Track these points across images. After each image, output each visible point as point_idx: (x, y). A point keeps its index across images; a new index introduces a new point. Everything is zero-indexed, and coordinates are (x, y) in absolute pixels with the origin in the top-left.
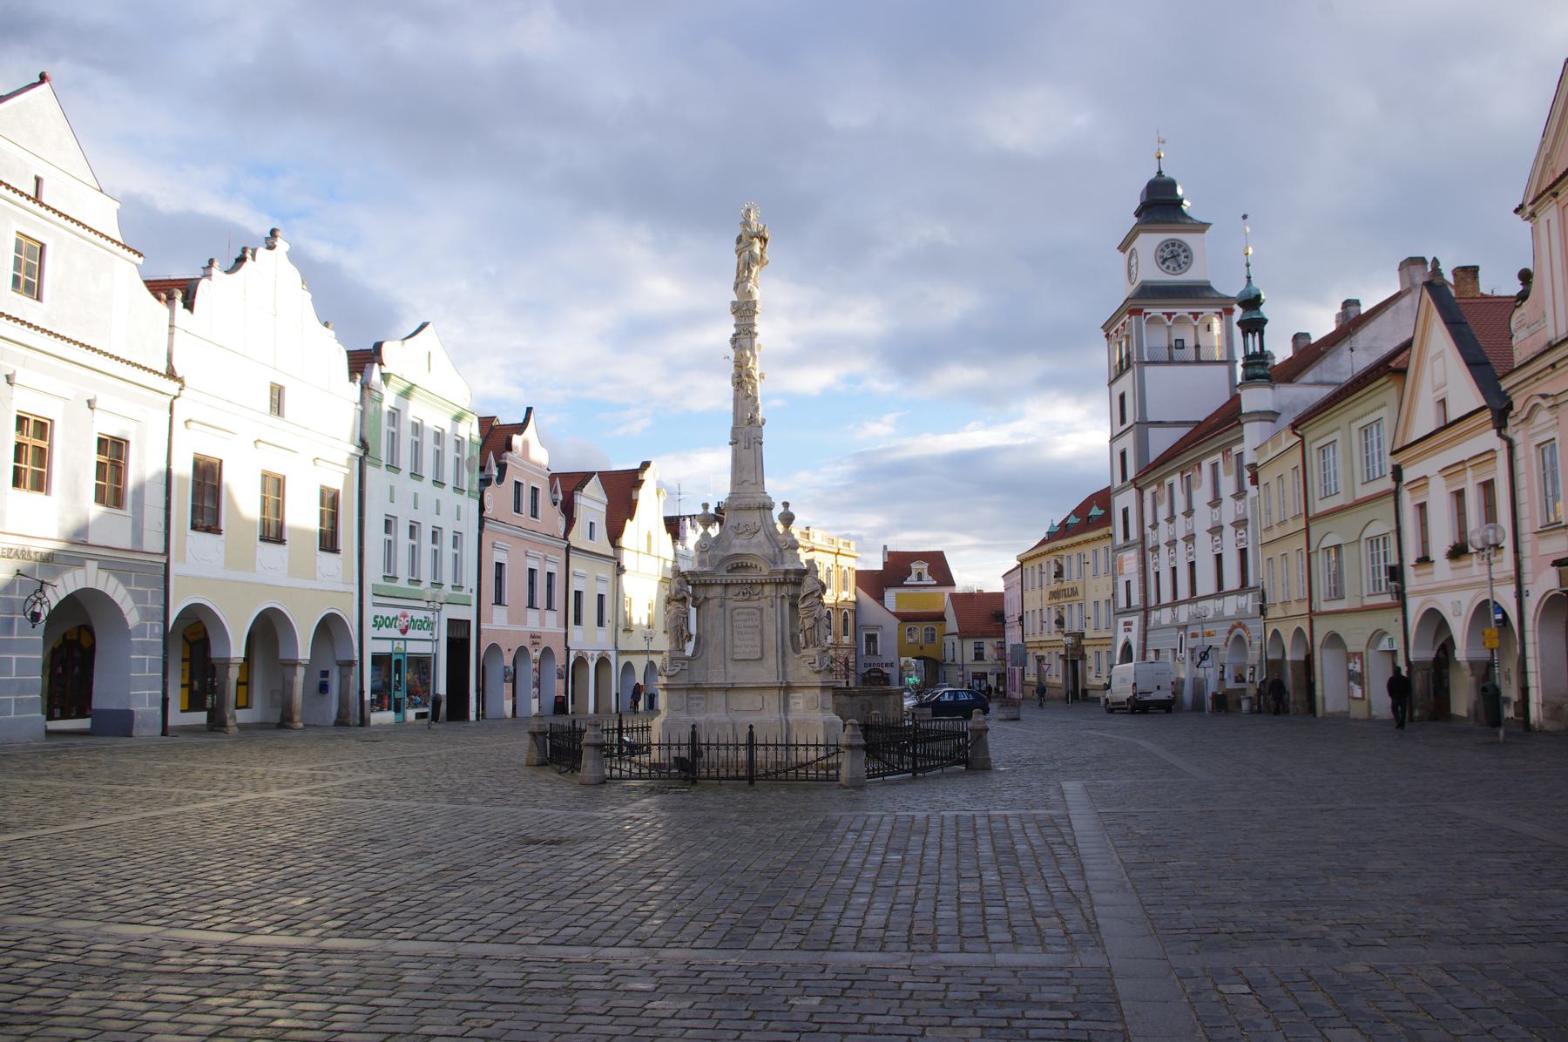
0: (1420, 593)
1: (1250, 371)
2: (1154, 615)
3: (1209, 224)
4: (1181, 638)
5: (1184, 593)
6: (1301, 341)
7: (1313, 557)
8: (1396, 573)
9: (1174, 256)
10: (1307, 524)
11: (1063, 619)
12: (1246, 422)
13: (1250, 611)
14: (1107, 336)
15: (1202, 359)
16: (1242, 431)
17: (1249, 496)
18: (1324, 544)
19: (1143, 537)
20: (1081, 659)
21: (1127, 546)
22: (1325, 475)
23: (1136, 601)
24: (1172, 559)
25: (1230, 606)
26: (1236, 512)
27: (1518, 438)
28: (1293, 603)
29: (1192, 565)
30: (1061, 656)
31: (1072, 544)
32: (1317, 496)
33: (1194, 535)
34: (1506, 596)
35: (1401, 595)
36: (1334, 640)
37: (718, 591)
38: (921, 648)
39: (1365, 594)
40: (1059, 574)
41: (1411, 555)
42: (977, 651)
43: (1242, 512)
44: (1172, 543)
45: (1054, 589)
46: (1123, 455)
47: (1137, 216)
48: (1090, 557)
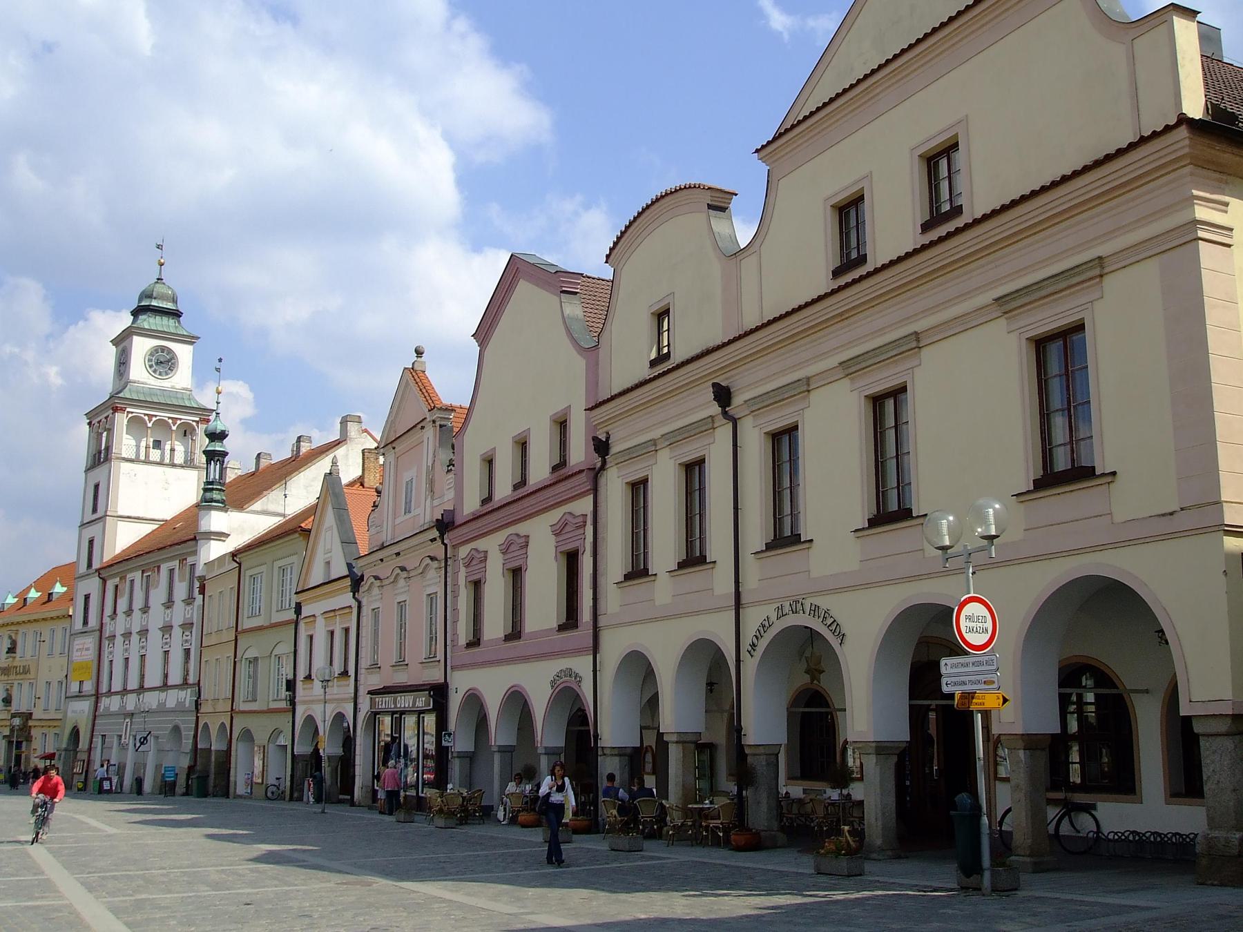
0: (305, 702)
1: (208, 495)
2: (104, 702)
4: (127, 725)
6: (262, 460)
8: (291, 685)
9: (163, 362)
10: (236, 637)
11: (11, 697)
12: (200, 539)
13: (187, 705)
14: (90, 424)
15: (176, 462)
19: (102, 624)
20: (27, 741)
21: (85, 632)
22: (253, 598)
23: (88, 687)
24: (126, 650)
25: (172, 699)
27: (364, 602)
29: (143, 656)
30: (5, 737)
31: (29, 621)
32: (246, 616)
33: (147, 630)
36: (247, 735)
39: (271, 699)
40: (12, 650)
41: (301, 674)
43: (189, 616)
44: (127, 635)
47: (132, 315)
48: (46, 635)
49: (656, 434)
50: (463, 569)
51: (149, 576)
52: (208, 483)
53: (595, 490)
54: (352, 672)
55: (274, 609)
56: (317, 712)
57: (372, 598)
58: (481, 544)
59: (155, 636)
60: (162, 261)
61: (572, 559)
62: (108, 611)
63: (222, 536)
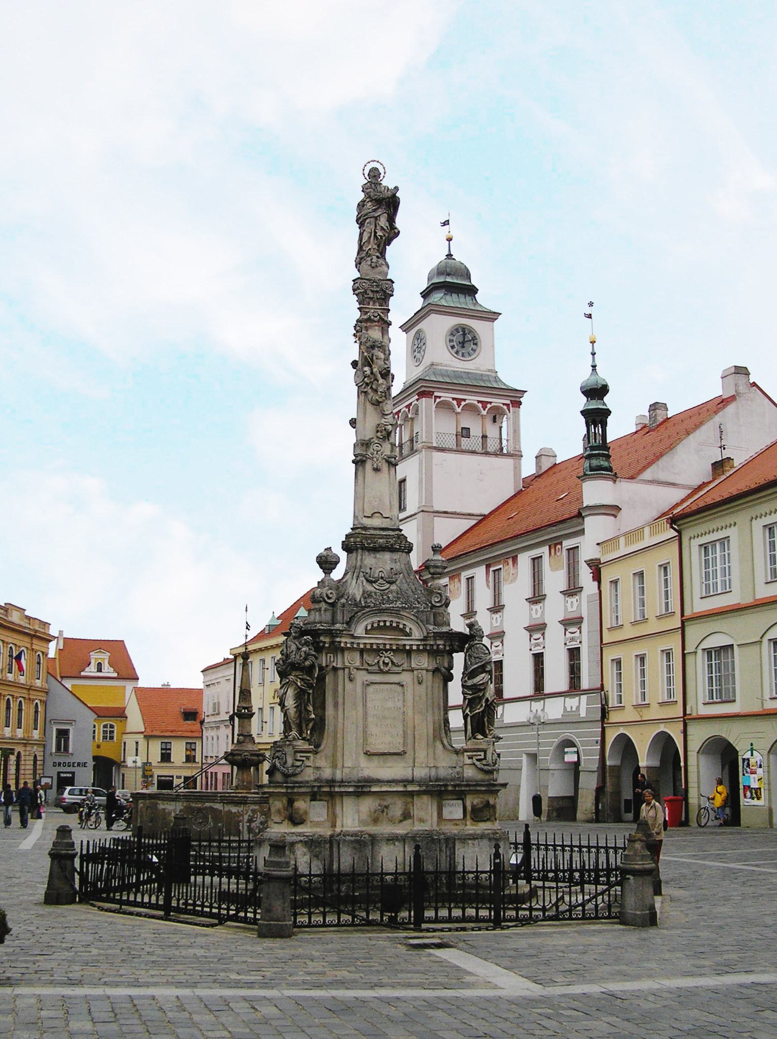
7: (689, 660)
10: (683, 622)
13: (583, 713)
15: (489, 450)
16: (583, 524)
17: (584, 594)
18: (707, 644)
25: (554, 709)
26: (566, 607)
28: (654, 706)
32: (697, 595)
38: (98, 747)
39: (767, 696)
42: (164, 751)
51: (501, 569)
60: (450, 236)
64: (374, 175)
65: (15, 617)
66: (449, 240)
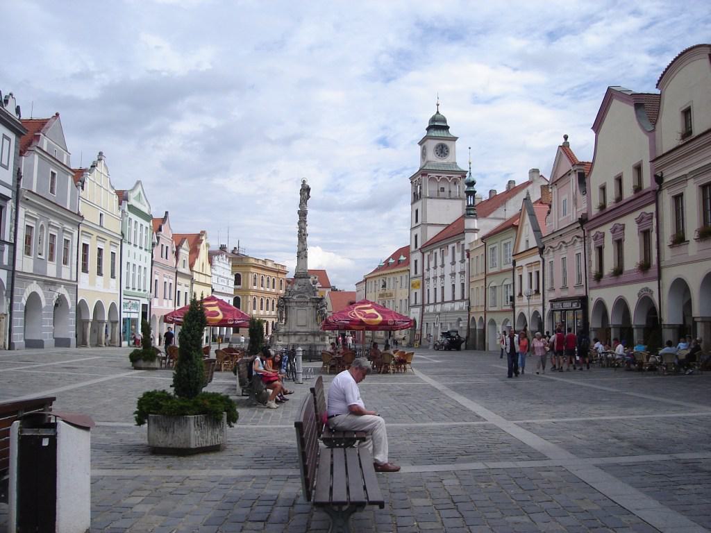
0: (519, 306)
1: (469, 212)
2: (426, 308)
3: (457, 138)
5: (439, 300)
8: (512, 299)
9: (442, 150)
14: (411, 182)
18: (492, 285)
23: (419, 301)
25: (457, 306)
27: (546, 258)
29: (443, 287)
34: (540, 309)
35: (513, 306)
36: (493, 322)
37: (294, 304)
40: (384, 286)
44: (435, 278)
45: (381, 293)
46: (416, 236)
48: (399, 279)
49: (686, 172)
50: (593, 242)
52: (468, 206)
53: (656, 201)
54: (541, 291)
55: (503, 263)
56: (525, 311)
57: (549, 257)
58: (601, 229)
59: (448, 277)
61: (646, 234)
62: (426, 267)
63: (475, 231)
64: (304, 182)
65: (269, 265)
66: (438, 105)
